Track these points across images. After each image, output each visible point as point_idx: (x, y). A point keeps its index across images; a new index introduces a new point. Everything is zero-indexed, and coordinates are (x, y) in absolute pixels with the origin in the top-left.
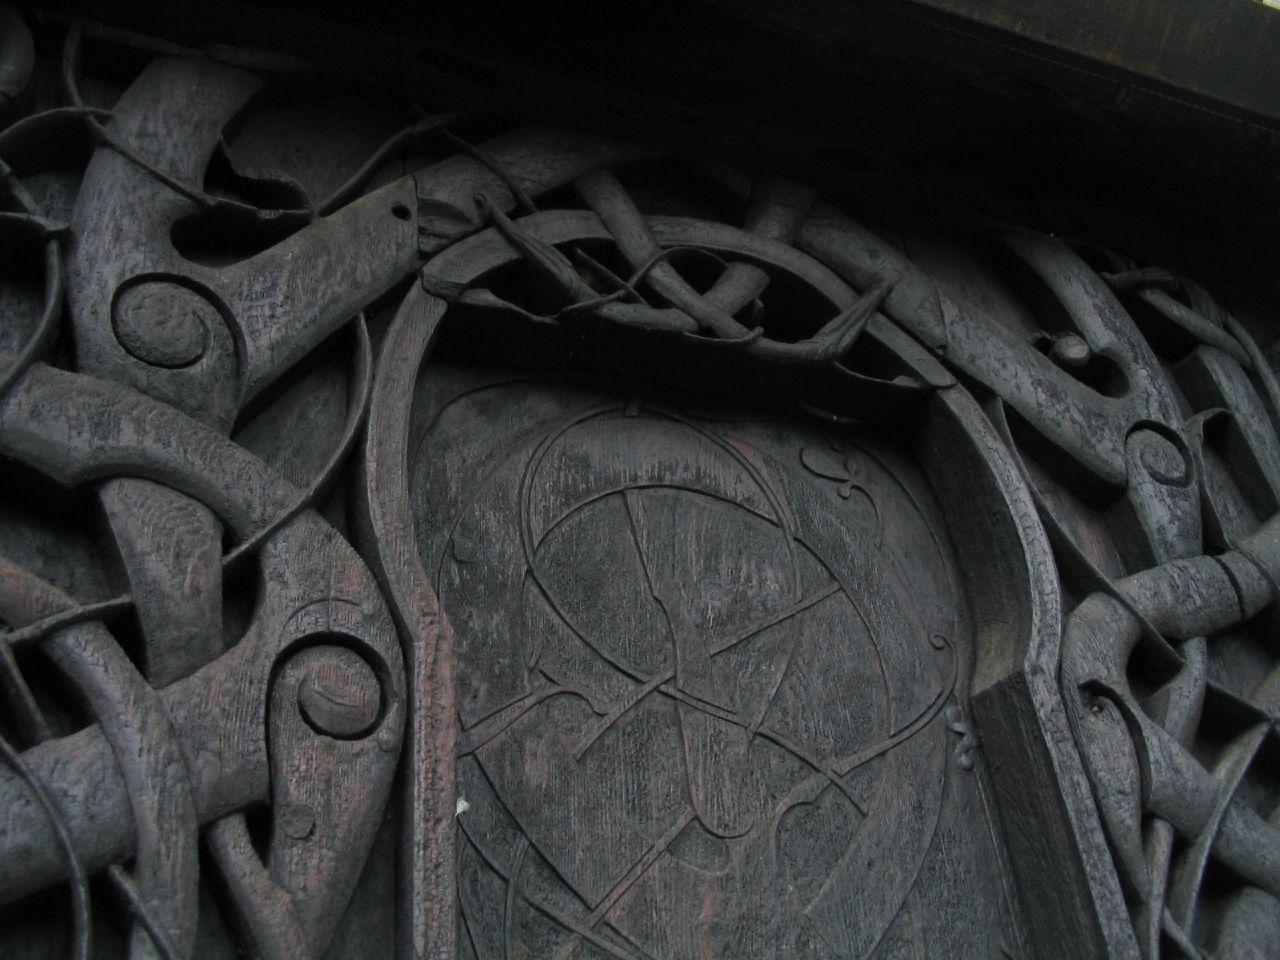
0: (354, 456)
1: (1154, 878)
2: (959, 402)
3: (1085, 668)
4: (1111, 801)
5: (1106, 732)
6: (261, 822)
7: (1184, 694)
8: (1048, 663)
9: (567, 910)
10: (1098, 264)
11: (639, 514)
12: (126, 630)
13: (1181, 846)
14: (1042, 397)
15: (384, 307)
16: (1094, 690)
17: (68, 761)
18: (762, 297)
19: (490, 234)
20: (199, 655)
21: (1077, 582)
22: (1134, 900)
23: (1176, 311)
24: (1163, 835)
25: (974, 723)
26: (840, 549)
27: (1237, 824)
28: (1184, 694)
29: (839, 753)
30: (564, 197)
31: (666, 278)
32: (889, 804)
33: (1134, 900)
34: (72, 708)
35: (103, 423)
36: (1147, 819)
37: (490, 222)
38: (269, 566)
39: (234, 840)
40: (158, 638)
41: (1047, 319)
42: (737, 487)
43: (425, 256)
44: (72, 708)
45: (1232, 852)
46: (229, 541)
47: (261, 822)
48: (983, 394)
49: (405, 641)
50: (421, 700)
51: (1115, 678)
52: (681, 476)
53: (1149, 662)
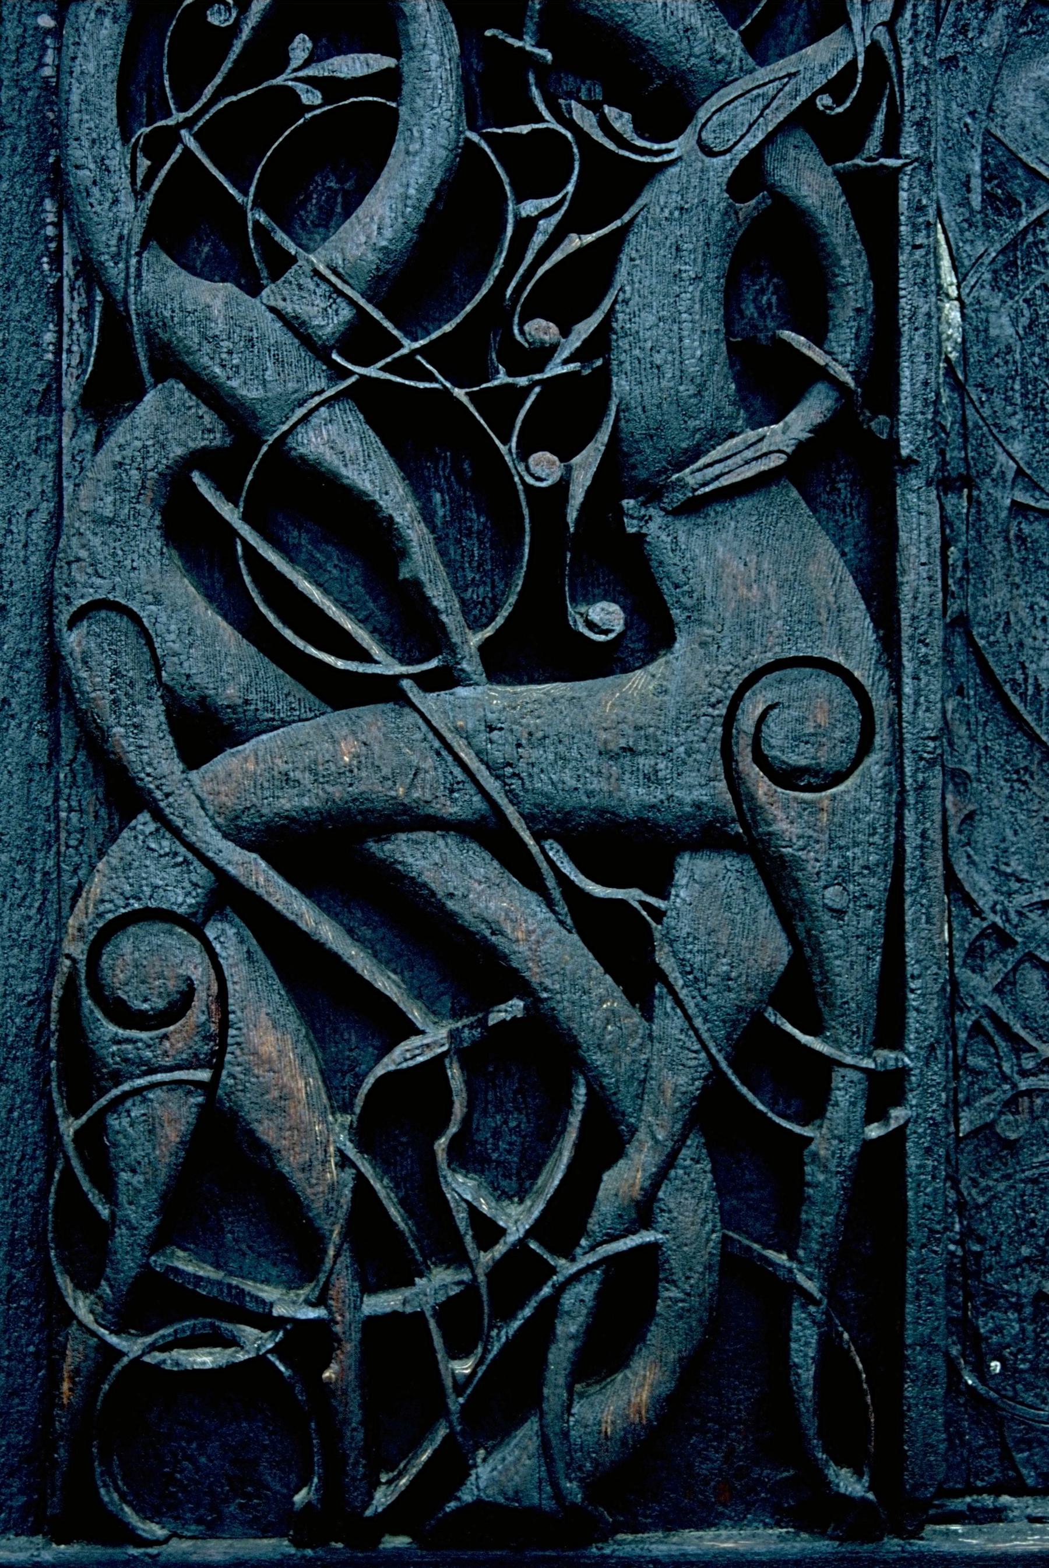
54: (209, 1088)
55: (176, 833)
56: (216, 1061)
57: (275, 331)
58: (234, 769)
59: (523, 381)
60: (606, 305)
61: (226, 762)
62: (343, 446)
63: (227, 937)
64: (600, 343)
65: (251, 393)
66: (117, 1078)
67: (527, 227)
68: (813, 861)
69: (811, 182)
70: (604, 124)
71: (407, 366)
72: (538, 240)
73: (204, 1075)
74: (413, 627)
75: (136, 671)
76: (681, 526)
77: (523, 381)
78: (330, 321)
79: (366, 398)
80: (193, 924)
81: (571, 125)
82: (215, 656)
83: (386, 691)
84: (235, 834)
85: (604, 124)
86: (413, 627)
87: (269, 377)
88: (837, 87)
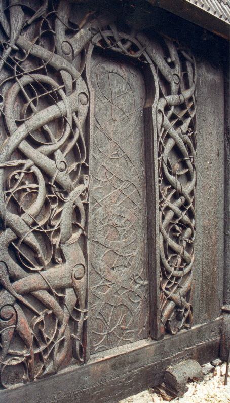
0: (85, 69)
1: (160, 135)
2: (152, 67)
3: (159, 108)
4: (158, 124)
5: (160, 116)
6: (77, 113)
7: (170, 113)
8: (155, 106)
9: (99, 127)
10: (176, 45)
11: (110, 76)
12: (64, 89)
13: (165, 131)
14: (163, 68)
15: (87, 46)
16: (160, 111)
17: (60, 103)
18: (131, 47)
19: (99, 34)
20: (71, 93)
21: (161, 96)
22: (158, 137)
23: (185, 55)
24: (163, 129)
25: (144, 111)
26: (132, 84)
27: (171, 130)
28: (170, 113)
29: (128, 112)
30: (109, 29)
31: (119, 43)
32: (133, 119)
33: (158, 137)
34: (60, 99)
35: (61, 62)
36: (162, 127)
37: (99, 32)
38: (77, 83)
39: (74, 114)
40: (68, 91)
41: (167, 55)
42: (121, 74)
43: (92, 37)
44: (60, 99)
45: (170, 133)
46: (73, 79)
47: (77, 113)
48: (155, 66)
49: (89, 94)
50: (91, 101)
51: (162, 110)
52: (115, 71)
53: (167, 108)
54: (15, 328)
55: (11, 293)
56: (16, 323)
57: (24, 223)
58: (17, 283)
59: (52, 230)
60: (60, 220)
61: (16, 283)
62: (31, 239)
63: (17, 306)
64: (59, 225)
65: (21, 232)
66: (3, 328)
67: (52, 209)
68: (80, 289)
69: (80, 204)
70: (61, 195)
71: (39, 228)
72: (54, 211)
73: (14, 326)
74: (39, 262)
75: (6, 271)
76: (67, 248)
77: (52, 230)
78: (30, 221)
79: (34, 232)
80: (12, 306)
81: (58, 196)
82: (16, 268)
83: (37, 272)
84: (18, 293)
85: (61, 195)
86: (39, 262)
87: (23, 228)
88: (83, 192)
